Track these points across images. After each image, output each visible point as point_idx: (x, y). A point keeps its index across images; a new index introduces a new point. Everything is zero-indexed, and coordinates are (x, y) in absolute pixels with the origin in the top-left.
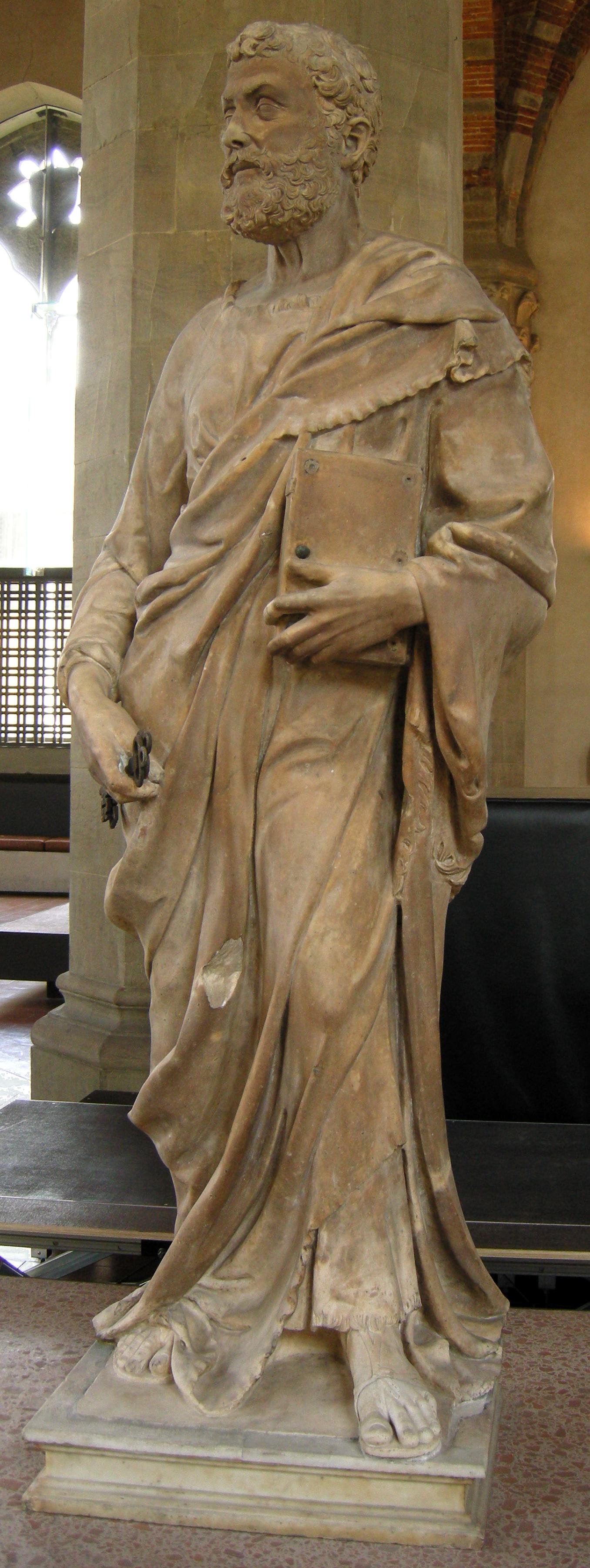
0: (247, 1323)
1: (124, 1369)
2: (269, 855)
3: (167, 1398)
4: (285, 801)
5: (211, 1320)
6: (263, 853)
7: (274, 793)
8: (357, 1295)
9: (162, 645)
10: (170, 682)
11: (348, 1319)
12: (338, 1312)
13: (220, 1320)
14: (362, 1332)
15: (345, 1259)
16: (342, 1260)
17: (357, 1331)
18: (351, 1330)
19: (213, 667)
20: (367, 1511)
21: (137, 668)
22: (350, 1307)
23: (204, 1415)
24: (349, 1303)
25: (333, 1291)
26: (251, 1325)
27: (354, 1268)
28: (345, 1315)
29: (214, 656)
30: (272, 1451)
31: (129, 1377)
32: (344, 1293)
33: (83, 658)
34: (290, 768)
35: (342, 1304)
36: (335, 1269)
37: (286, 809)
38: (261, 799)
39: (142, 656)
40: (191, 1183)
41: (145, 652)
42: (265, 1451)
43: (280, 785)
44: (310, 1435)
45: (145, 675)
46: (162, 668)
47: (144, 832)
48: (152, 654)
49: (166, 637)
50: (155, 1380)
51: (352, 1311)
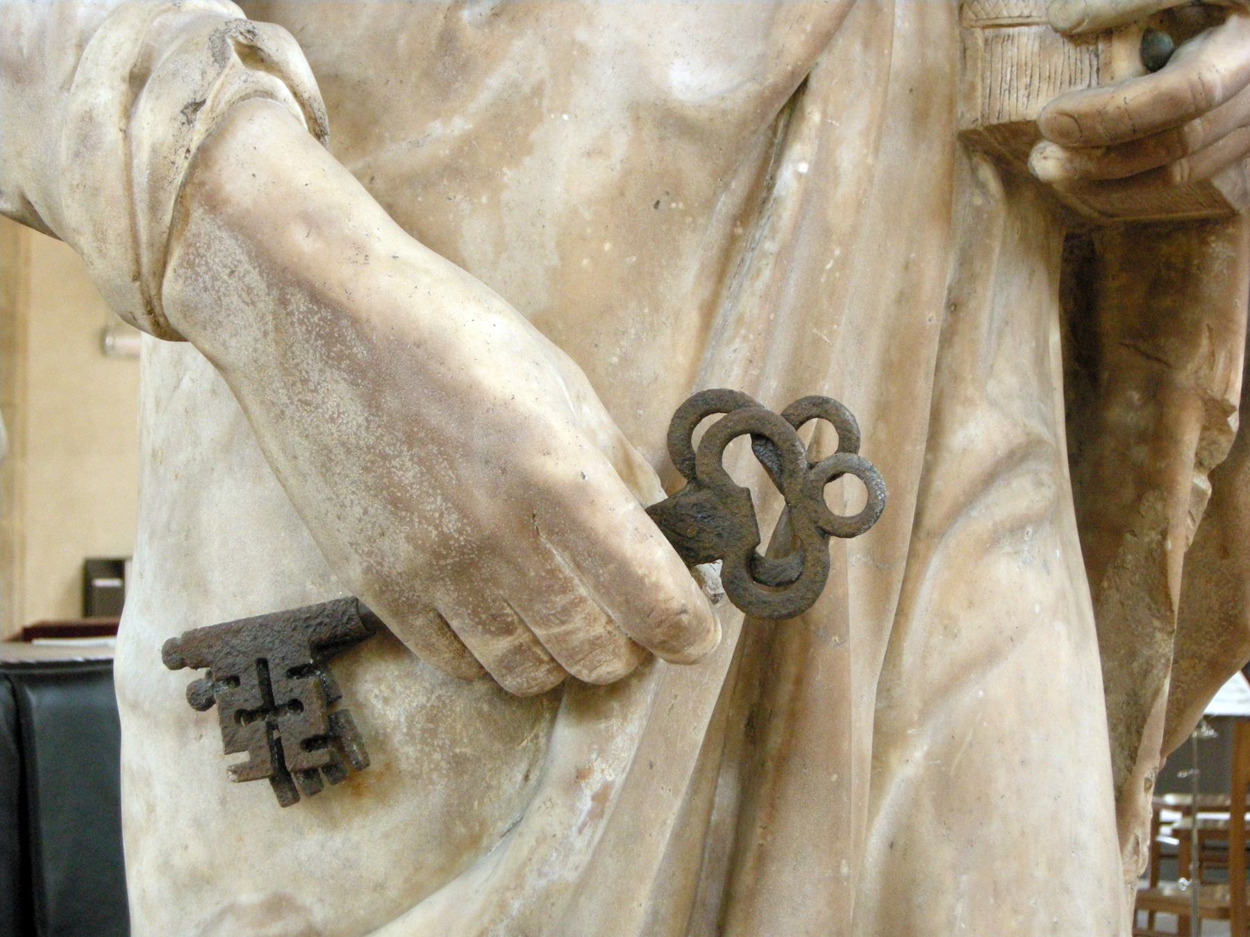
2: (940, 856)
4: (990, 656)
6: (901, 849)
7: (950, 632)
9: (572, 59)
10: (647, 208)
19: (823, 167)
21: (467, 144)
29: (825, 126)
33: (264, 78)
34: (992, 542)
37: (995, 685)
38: (908, 658)
39: (484, 97)
41: (494, 82)
43: (971, 604)
45: (508, 174)
46: (592, 153)
47: (601, 798)
48: (538, 91)
49: (581, 34)
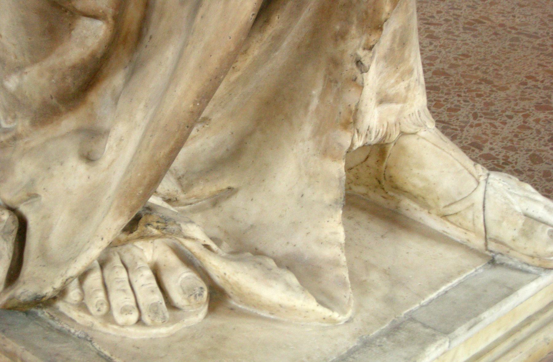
0: (224, 184)
1: (140, 321)
3: (243, 331)
5: (169, 201)
8: (408, 88)
11: (398, 123)
12: (381, 120)
13: (182, 196)
14: (422, 133)
15: (395, 46)
16: (391, 50)
17: (414, 134)
18: (403, 134)
20: (518, 336)
22: (399, 106)
23: (334, 322)
24: (397, 103)
25: (378, 94)
26: (232, 185)
27: (406, 54)
28: (392, 119)
30: (473, 321)
31: (163, 331)
32: (391, 92)
35: (386, 107)
36: (382, 63)
40: (110, 11)
42: (468, 324)
44: (455, 281)
50: (196, 315)
51: (401, 111)
